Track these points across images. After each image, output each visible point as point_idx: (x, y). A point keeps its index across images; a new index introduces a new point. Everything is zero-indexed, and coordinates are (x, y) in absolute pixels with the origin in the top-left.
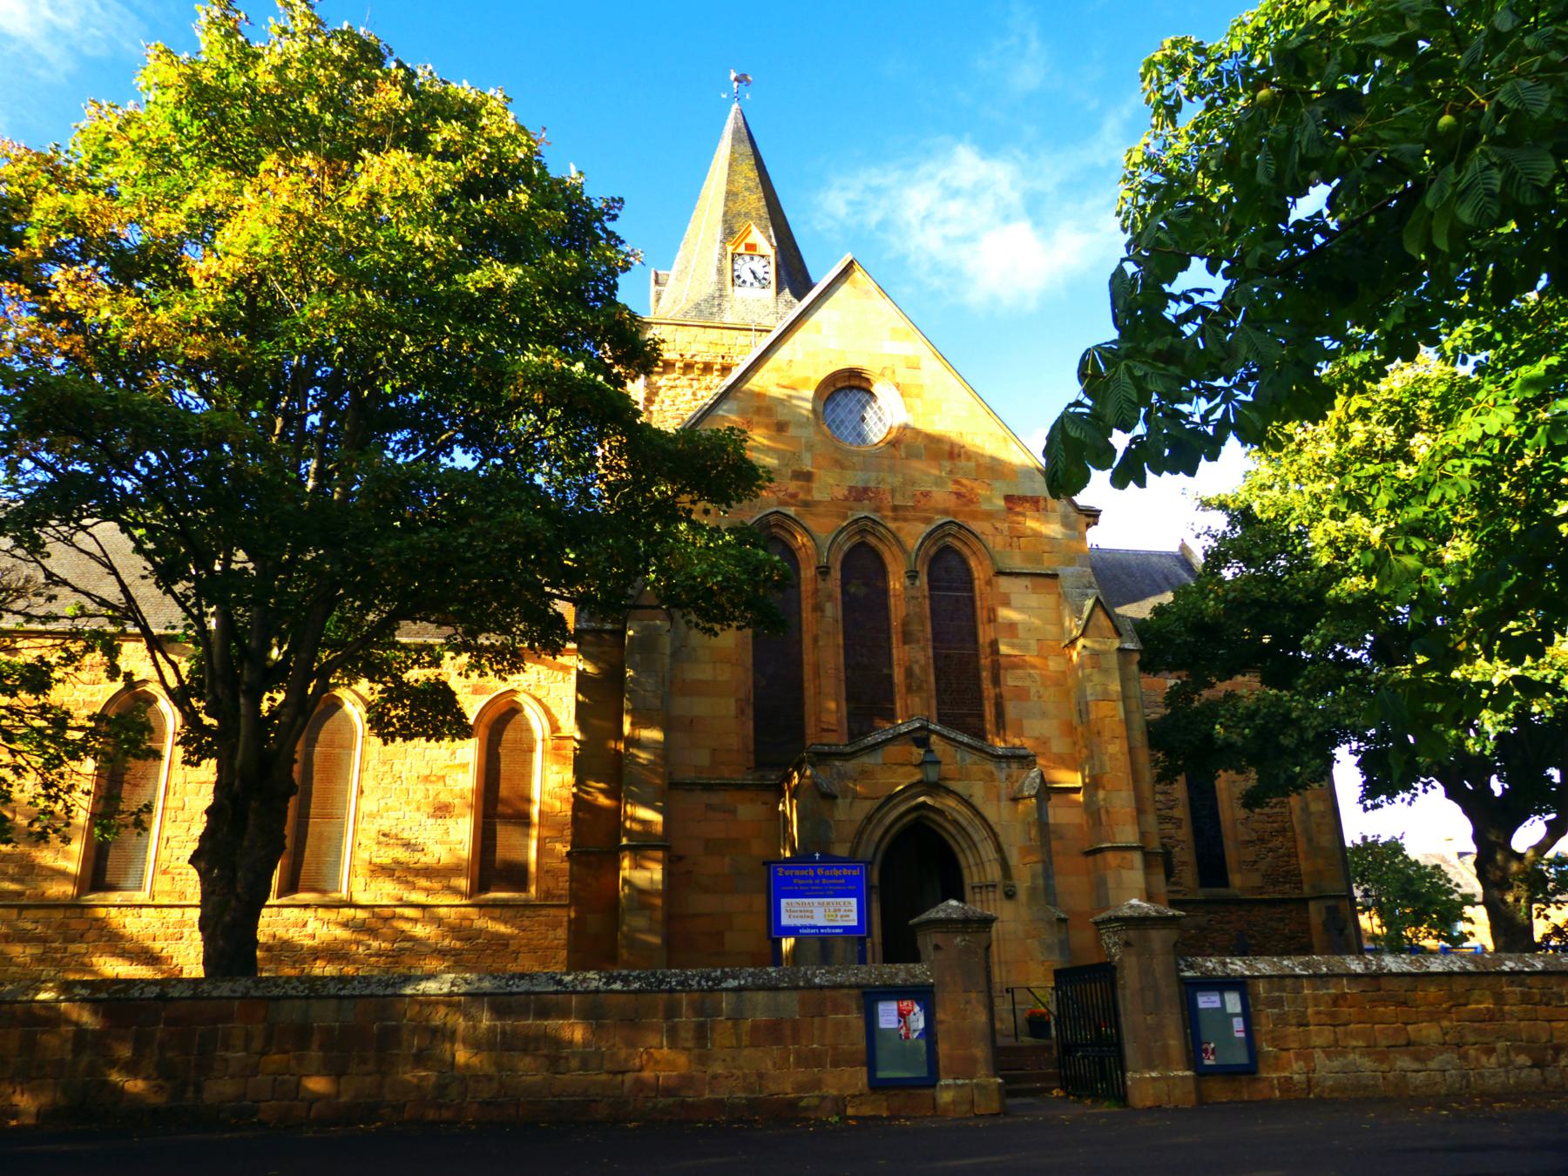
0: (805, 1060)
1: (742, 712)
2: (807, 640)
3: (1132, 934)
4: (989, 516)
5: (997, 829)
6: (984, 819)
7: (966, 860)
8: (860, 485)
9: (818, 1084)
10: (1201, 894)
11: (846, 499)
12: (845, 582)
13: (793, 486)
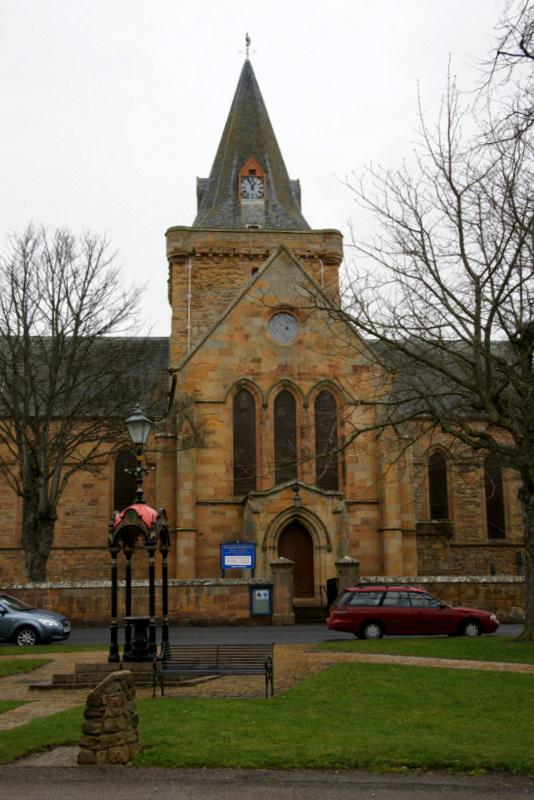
0: (230, 608)
1: (228, 471)
2: (258, 436)
3: (343, 569)
4: (344, 376)
5: (326, 525)
6: (320, 521)
7: (314, 536)
8: (284, 364)
9: (233, 615)
10: (487, 541)
11: (277, 371)
12: (275, 411)
13: (252, 366)
